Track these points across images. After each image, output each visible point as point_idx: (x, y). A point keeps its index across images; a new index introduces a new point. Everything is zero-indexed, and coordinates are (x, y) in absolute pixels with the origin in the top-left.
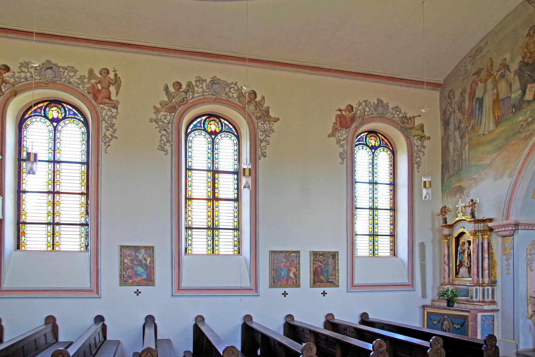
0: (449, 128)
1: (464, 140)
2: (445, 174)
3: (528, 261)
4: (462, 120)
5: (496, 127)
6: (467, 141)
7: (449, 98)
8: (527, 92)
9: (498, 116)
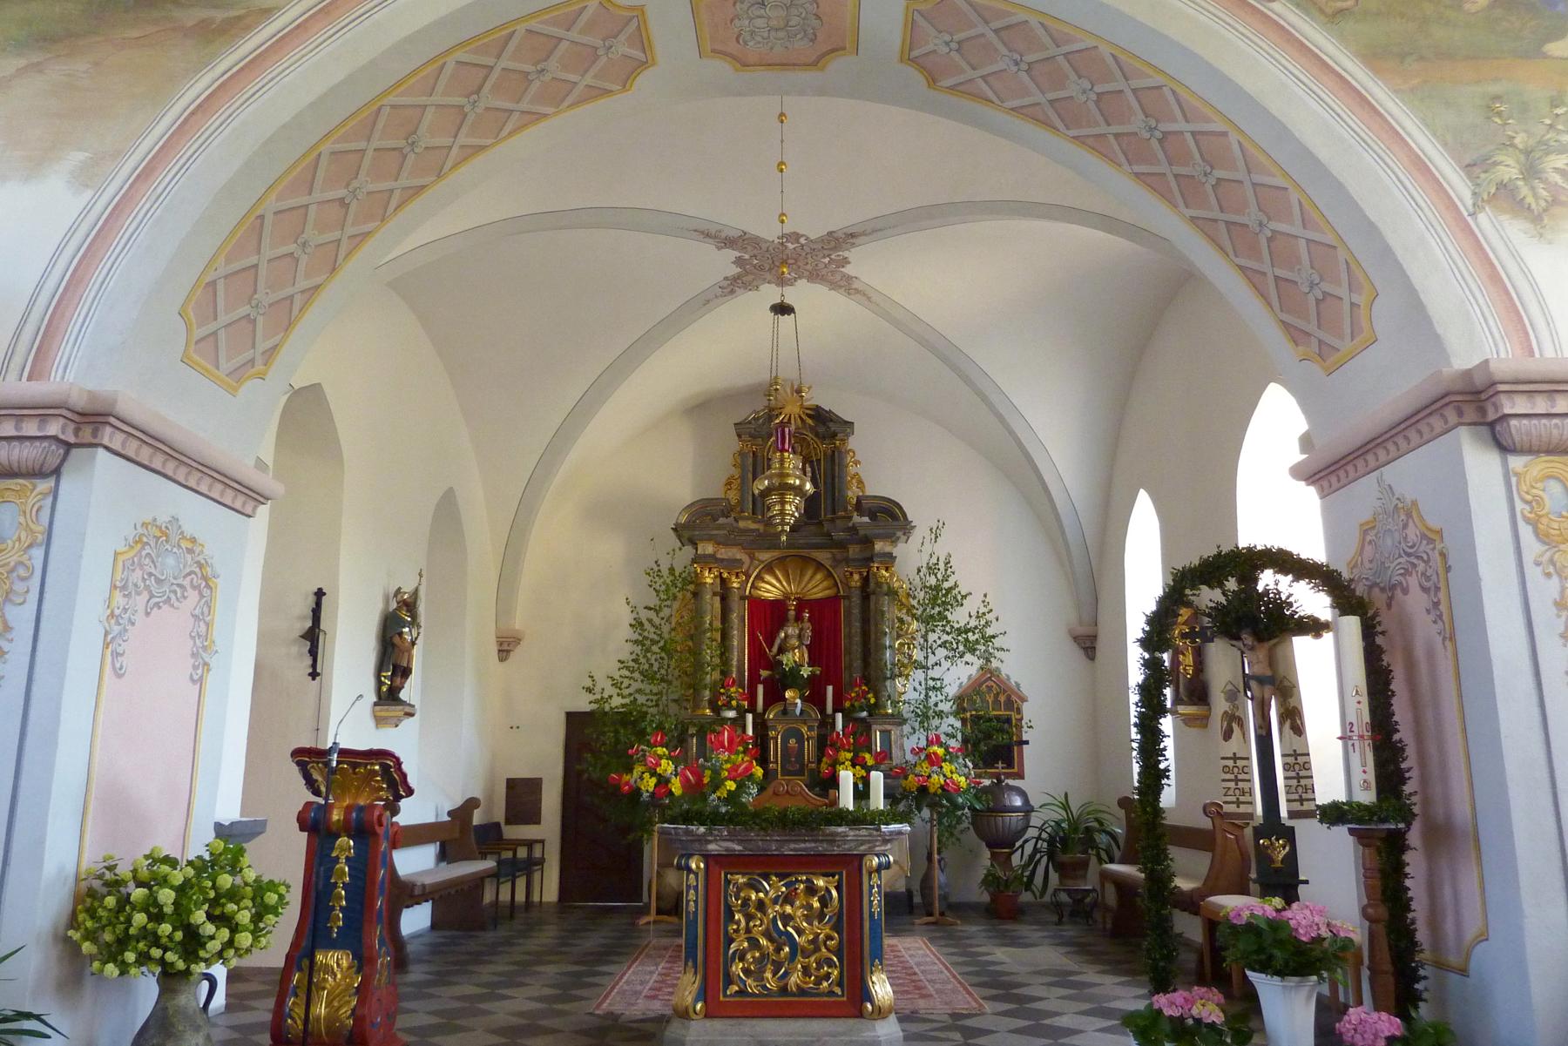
3: (113, 621)
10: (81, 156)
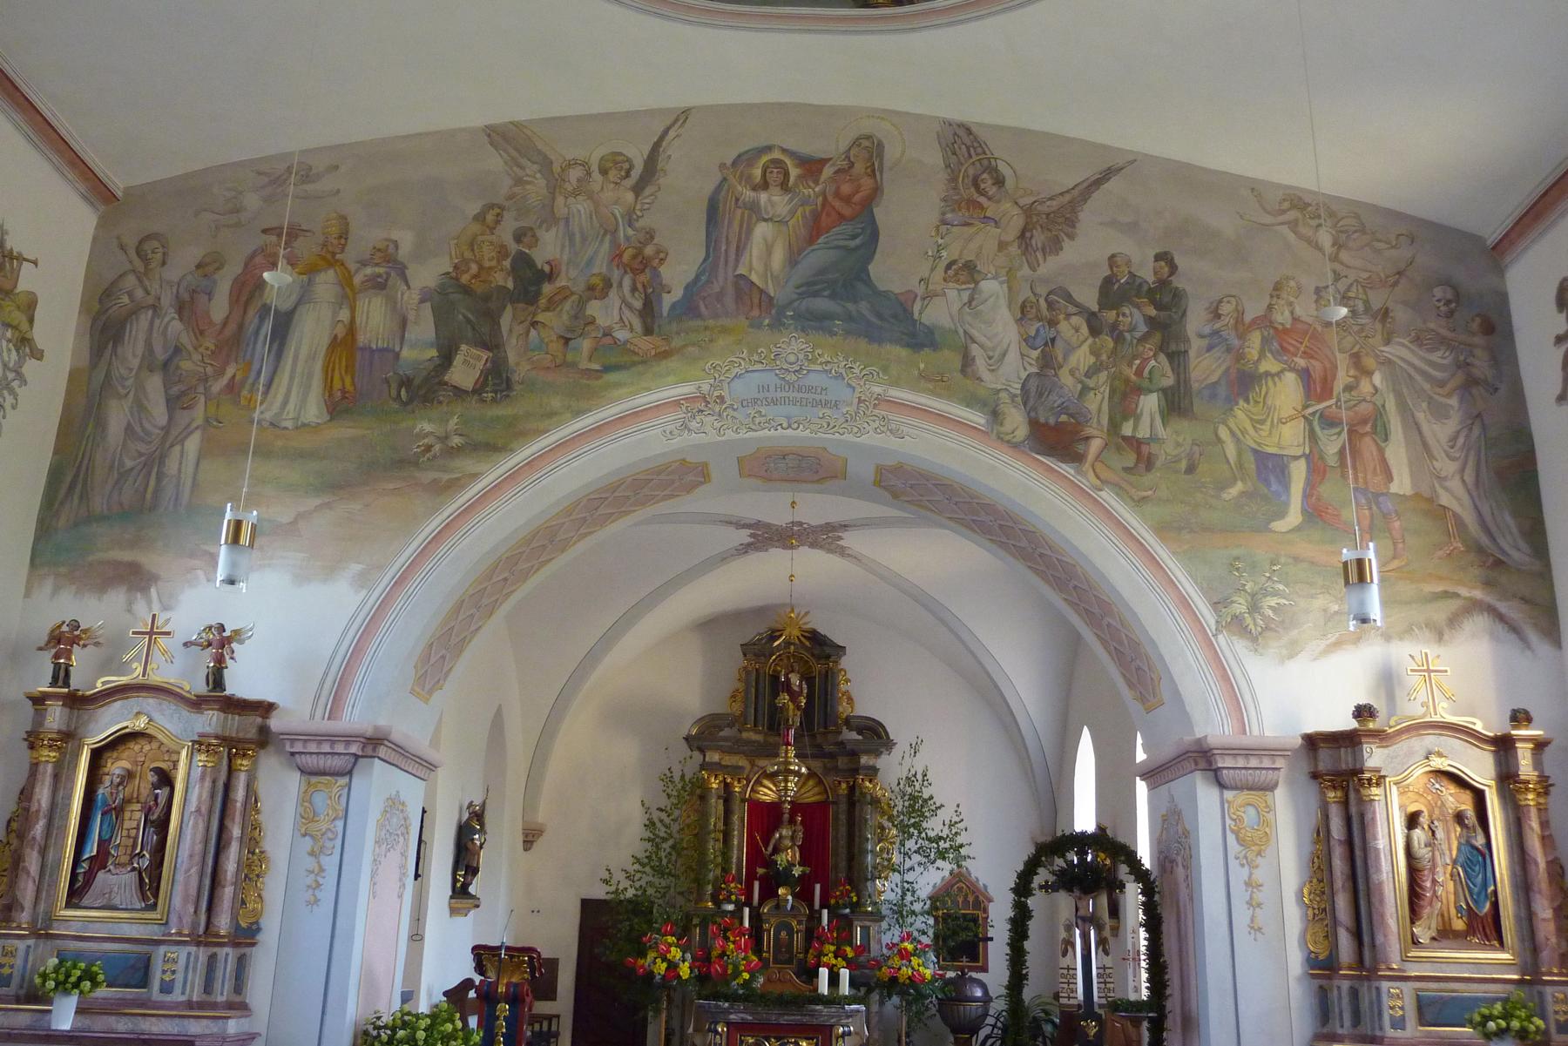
0: (119, 350)
1: (183, 418)
2: (62, 503)
4: (191, 349)
5: (331, 420)
6: (199, 421)
7: (138, 254)
8: (455, 363)
9: (343, 391)
10: (356, 568)
